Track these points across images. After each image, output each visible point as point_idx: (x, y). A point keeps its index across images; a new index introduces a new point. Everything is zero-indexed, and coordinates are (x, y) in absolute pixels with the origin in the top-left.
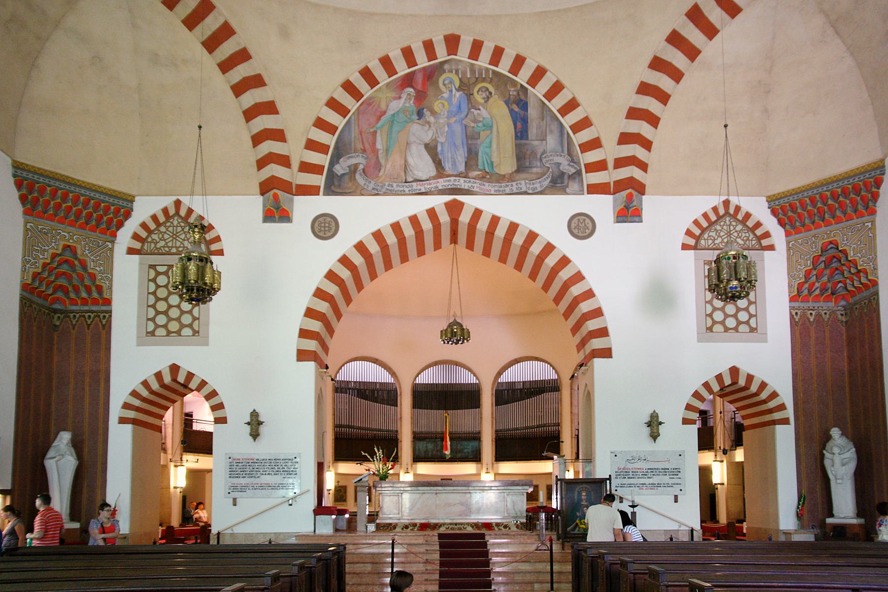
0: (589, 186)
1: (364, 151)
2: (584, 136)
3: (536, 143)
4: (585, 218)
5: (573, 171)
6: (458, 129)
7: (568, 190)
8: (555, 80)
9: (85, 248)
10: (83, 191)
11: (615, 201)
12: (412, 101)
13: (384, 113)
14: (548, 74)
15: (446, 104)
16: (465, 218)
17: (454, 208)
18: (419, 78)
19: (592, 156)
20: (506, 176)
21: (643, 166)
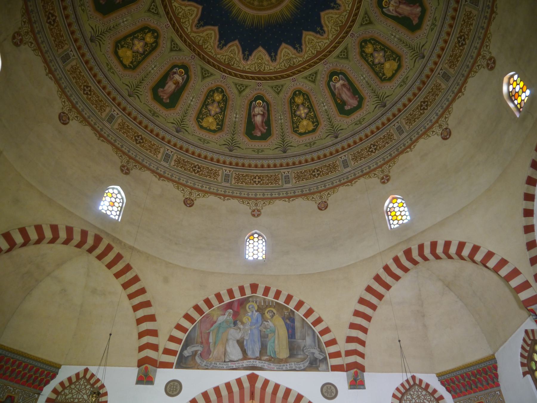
0: (332, 366)
1: (202, 343)
2: (327, 338)
3: (300, 341)
4: (331, 386)
5: (322, 357)
6: (256, 332)
7: (319, 369)
8: (309, 307)
9: (20, 398)
10: (18, 357)
11: (348, 376)
12: (231, 317)
13: (215, 322)
14: (305, 304)
15: (250, 318)
16: (259, 385)
17: (253, 379)
18: (236, 305)
19: (332, 349)
20: (283, 360)
21: (362, 355)
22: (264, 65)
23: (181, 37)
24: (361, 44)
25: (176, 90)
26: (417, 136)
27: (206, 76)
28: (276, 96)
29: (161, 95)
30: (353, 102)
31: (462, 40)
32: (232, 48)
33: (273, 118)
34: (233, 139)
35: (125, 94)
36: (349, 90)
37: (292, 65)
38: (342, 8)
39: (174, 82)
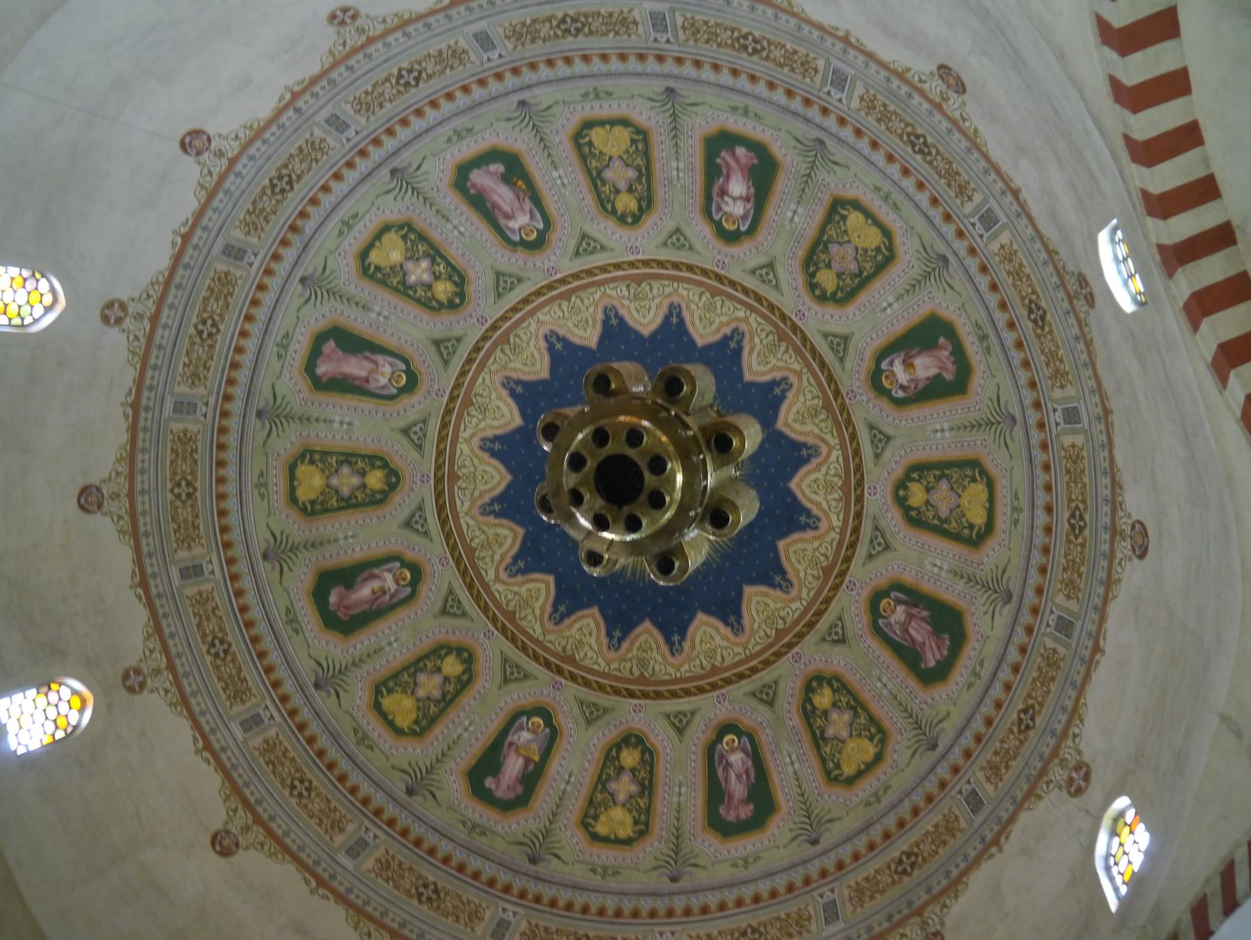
22: (701, 304)
23: (857, 452)
24: (462, 301)
25: (915, 352)
26: (283, 119)
27: (838, 340)
28: (683, 227)
29: (954, 363)
30: (479, 178)
31: (208, 330)
32: (762, 368)
33: (698, 179)
34: (812, 166)
35: (1018, 431)
36: (495, 206)
37: (633, 284)
38: (498, 379)
39: (912, 371)
